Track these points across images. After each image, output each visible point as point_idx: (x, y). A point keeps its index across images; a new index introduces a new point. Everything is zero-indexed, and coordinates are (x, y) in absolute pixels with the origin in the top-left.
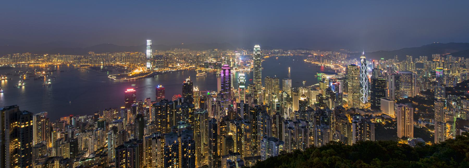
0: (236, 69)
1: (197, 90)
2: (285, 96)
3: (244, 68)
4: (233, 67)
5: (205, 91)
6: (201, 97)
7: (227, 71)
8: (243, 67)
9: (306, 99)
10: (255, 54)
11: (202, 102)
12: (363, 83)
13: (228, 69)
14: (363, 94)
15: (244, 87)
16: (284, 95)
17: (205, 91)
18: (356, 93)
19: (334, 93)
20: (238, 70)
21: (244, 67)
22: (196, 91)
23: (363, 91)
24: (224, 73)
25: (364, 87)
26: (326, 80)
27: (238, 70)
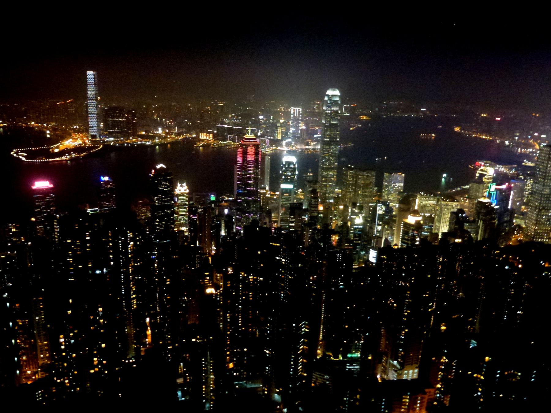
0: (288, 145)
1: (185, 190)
2: (381, 210)
3: (307, 144)
4: (282, 140)
5: (204, 194)
6: (192, 206)
7: (251, 150)
8: (306, 139)
9: (420, 221)
10: (327, 112)
11: (192, 216)
13: (254, 145)
15: (290, 186)
16: (378, 208)
17: (204, 194)
19: (496, 207)
20: (293, 146)
21: (307, 140)
22: (182, 191)
24: (245, 153)
26: (486, 177)
27: (294, 148)
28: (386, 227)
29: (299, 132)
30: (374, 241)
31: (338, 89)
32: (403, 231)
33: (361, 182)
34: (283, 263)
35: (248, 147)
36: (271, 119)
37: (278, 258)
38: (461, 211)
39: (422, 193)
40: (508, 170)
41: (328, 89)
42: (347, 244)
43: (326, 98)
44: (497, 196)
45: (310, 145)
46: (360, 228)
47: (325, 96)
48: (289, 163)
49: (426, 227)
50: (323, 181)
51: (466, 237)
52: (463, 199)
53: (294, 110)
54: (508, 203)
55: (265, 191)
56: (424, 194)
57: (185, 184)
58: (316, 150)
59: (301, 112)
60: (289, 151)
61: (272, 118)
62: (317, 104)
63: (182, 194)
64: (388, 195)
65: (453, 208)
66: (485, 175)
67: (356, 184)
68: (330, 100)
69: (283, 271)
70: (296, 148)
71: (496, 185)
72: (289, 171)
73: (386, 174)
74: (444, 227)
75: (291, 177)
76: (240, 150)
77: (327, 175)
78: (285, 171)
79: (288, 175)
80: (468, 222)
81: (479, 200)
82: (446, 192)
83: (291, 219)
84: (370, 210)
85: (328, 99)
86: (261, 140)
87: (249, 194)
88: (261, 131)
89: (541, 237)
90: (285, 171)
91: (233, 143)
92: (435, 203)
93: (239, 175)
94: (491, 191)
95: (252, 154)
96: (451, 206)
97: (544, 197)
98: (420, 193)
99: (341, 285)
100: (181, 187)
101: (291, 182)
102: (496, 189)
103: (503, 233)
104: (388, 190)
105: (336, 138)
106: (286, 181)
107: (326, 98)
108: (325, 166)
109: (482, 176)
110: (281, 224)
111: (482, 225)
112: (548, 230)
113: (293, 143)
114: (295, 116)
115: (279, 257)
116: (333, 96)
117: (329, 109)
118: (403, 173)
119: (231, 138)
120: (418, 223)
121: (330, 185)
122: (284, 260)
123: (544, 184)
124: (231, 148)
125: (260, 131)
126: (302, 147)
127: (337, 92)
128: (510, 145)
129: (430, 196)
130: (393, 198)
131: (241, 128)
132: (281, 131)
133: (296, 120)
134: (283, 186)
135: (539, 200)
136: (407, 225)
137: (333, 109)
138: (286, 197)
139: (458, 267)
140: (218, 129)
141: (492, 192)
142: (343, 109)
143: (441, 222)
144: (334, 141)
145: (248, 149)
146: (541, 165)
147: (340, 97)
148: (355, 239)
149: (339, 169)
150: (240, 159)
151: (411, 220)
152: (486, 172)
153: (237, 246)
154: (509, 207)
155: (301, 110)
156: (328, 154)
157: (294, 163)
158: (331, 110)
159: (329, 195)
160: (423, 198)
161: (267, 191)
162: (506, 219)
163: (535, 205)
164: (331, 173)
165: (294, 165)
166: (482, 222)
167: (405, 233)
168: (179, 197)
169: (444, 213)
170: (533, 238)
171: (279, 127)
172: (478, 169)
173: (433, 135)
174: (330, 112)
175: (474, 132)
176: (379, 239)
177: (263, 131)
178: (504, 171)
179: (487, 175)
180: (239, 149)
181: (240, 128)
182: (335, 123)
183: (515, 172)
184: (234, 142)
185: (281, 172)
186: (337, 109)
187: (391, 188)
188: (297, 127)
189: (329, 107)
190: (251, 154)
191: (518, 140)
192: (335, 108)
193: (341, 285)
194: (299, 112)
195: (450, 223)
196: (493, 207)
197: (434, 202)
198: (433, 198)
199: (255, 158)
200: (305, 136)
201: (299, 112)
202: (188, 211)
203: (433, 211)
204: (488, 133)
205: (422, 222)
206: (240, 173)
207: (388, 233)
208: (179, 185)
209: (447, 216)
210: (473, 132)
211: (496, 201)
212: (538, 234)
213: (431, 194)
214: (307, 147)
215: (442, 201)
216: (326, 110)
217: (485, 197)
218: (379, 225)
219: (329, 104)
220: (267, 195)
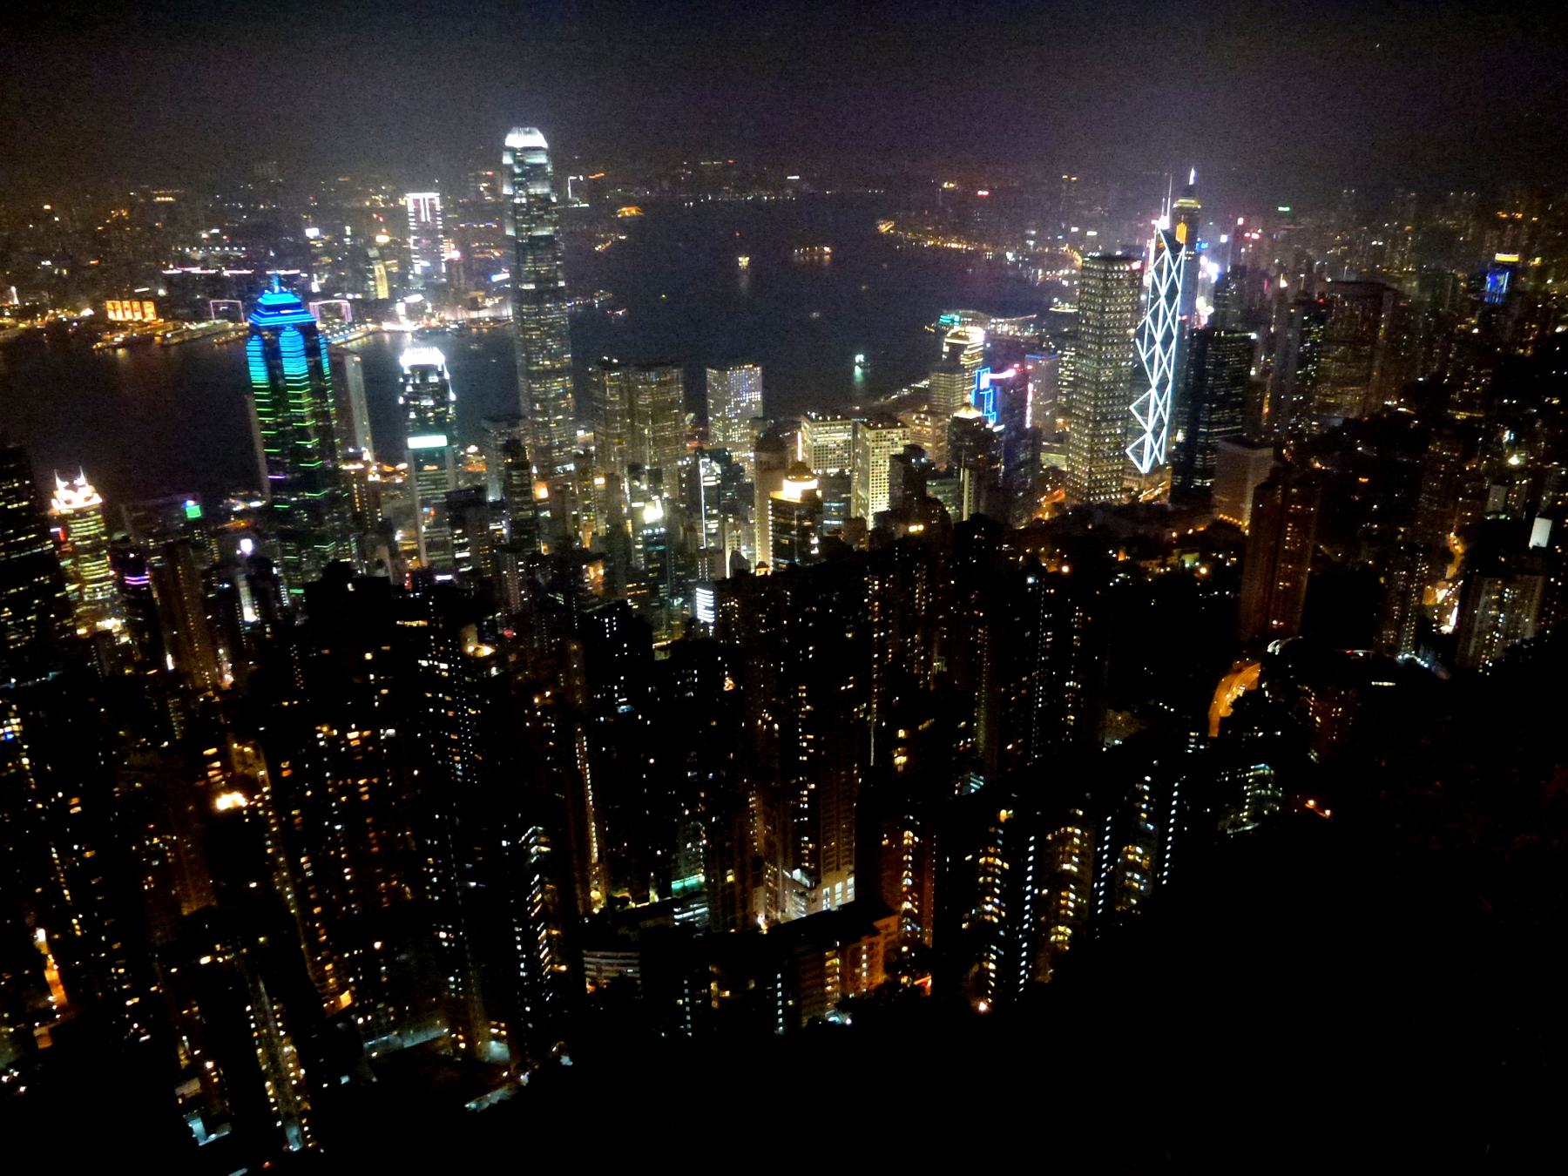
0: (414, 312)
1: (88, 499)
2: (709, 474)
3: (474, 305)
4: (390, 301)
6: (122, 547)
7: (290, 342)
8: (466, 291)
10: (517, 201)
11: (131, 580)
12: (1151, 360)
13: (295, 326)
15: (438, 441)
16: (702, 471)
18: (1112, 419)
19: (997, 429)
20: (432, 315)
21: (473, 294)
24: (272, 355)
25: (1154, 382)
26: (966, 352)
27: (434, 322)
28: (731, 520)
29: (444, 270)
30: (703, 565)
31: (541, 131)
32: (775, 524)
33: (645, 400)
34: (445, 674)
35: (278, 335)
36: (347, 237)
37: (424, 663)
38: (914, 450)
39: (813, 415)
40: (1019, 330)
41: (507, 130)
42: (630, 586)
43: (507, 160)
44: (998, 402)
45: (485, 308)
46: (660, 535)
47: (504, 153)
48: (424, 371)
50: (535, 413)
51: (933, 517)
52: (917, 418)
53: (416, 202)
54: (1023, 415)
55: (360, 466)
56: (817, 417)
57: (81, 480)
58: (504, 321)
59: (438, 208)
60: (421, 331)
61: (349, 233)
62: (487, 179)
63: (82, 514)
64: (725, 429)
65: (895, 444)
66: (964, 347)
67: (632, 412)
68: (521, 163)
69: (447, 698)
70: (440, 321)
71: (992, 372)
72: (427, 394)
73: (712, 373)
75: (437, 413)
76: (254, 347)
77: (546, 392)
78: (416, 395)
79: (426, 407)
80: (936, 476)
81: (956, 415)
82: (876, 403)
83: (458, 539)
84: (681, 481)
85: (515, 162)
86: (322, 305)
87: (310, 480)
88: (320, 278)
89: (1103, 490)
90: (416, 395)
91: (231, 325)
92: (850, 438)
93: (267, 427)
94: (982, 388)
95: (300, 353)
97: (1103, 390)
98: (806, 415)
99: (623, 703)
100: (71, 492)
101: (440, 426)
102: (993, 382)
103: (1021, 494)
104: (723, 418)
105: (556, 280)
106: (424, 427)
107: (507, 160)
108: (535, 368)
109: (957, 350)
110: (430, 559)
112: (1118, 471)
113: (429, 305)
114: (423, 220)
115: (427, 659)
116: (527, 150)
117: (521, 192)
118: (755, 366)
119: (221, 309)
120: (809, 496)
121: (558, 422)
122: (444, 666)
123: (1100, 357)
124: (227, 342)
125: (315, 276)
126: (459, 317)
127: (538, 139)
128: (1018, 261)
130: (739, 438)
131: (249, 272)
132: (383, 272)
133: (427, 231)
134: (416, 443)
136: (781, 508)
137: (532, 191)
138: (429, 475)
139: (920, 599)
140: (170, 282)
141: (985, 390)
142: (569, 189)
144: (548, 291)
145: (281, 339)
146: (1090, 309)
147: (549, 153)
148: (651, 567)
149: (576, 371)
150: (258, 374)
151: (791, 491)
152: (966, 338)
153: (295, 649)
154: (1028, 425)
155: (437, 202)
156: (538, 329)
157: (440, 369)
158: (528, 196)
159: (560, 452)
160: (815, 426)
161: (367, 464)
162: (1022, 456)
163: (1085, 411)
164: (556, 386)
165: (440, 374)
166: (967, 472)
167: (781, 529)
168: (72, 526)
171: (375, 259)
172: (947, 332)
173: (827, 249)
174: (524, 201)
176: (718, 557)
177: (326, 276)
178: (1008, 332)
180: (252, 343)
181: (246, 272)
182: (545, 233)
183: (1034, 332)
184: (235, 319)
185: (401, 401)
186: (546, 190)
187: (730, 410)
188: (435, 257)
189: (521, 185)
190: (294, 354)
191: (1035, 247)
192: (540, 189)
193: (623, 703)
194: (432, 207)
195: (892, 486)
196: (991, 430)
197: (846, 436)
199: (309, 367)
200: (462, 281)
201: (432, 207)
202: (113, 566)
204: (959, 231)
205: (819, 494)
206: (267, 420)
207: (738, 537)
208: (60, 484)
209: (882, 469)
210: (927, 234)
211: (995, 413)
212: (1096, 483)
213: (834, 414)
214: (474, 315)
215: (866, 430)
216: (513, 197)
217: (967, 405)
218: (710, 517)
219: (519, 175)
220: (371, 478)
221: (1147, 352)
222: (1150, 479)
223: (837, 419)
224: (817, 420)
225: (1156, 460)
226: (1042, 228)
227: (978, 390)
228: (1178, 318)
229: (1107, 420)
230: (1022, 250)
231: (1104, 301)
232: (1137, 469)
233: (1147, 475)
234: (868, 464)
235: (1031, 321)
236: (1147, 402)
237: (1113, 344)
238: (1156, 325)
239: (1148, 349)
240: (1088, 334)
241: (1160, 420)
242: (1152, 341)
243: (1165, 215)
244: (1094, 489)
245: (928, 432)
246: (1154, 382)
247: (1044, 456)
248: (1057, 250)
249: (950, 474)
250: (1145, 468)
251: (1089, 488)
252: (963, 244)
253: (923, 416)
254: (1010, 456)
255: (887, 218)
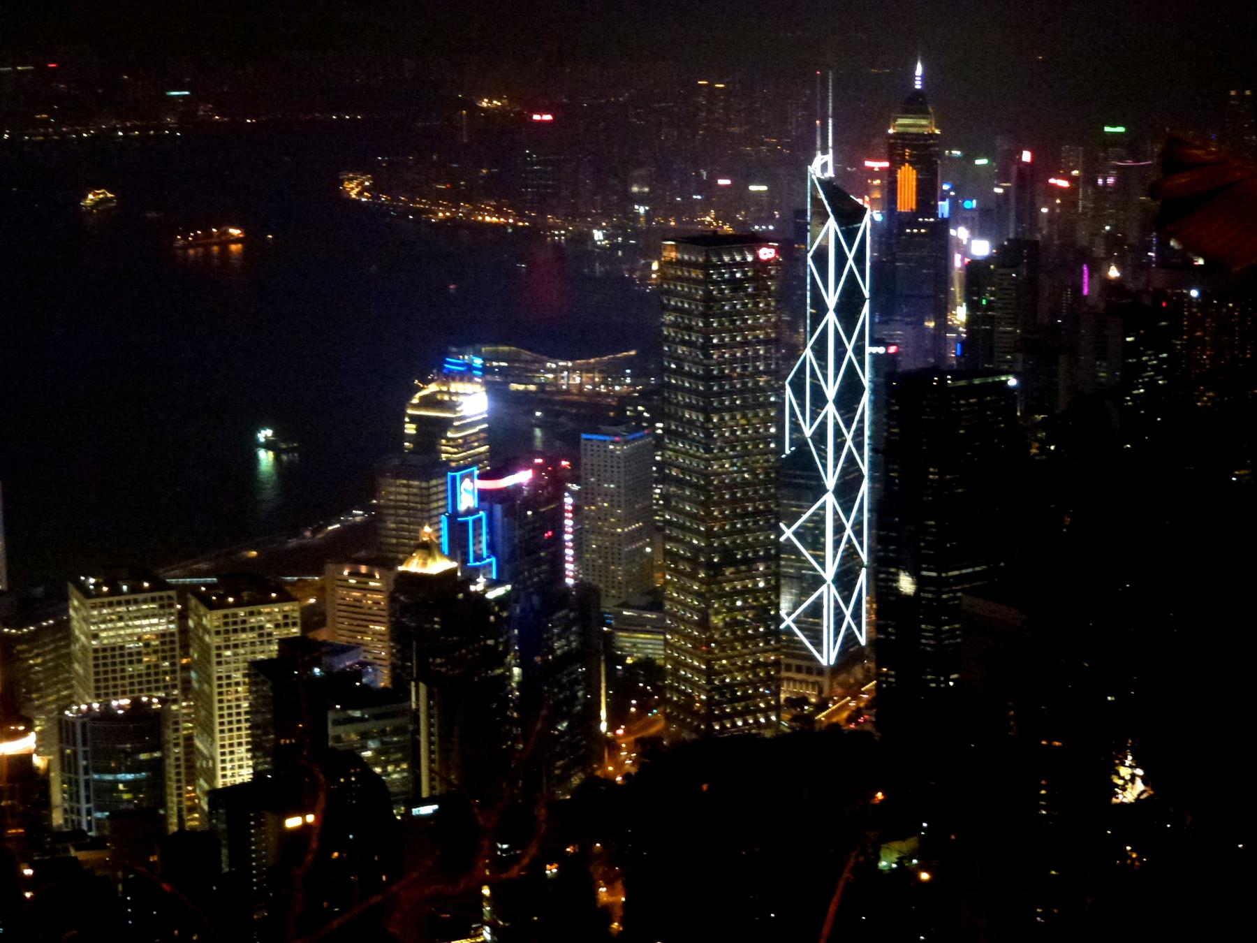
12: (820, 435)
14: (823, 565)
18: (745, 560)
23: (823, 520)
25: (830, 482)
39: (92, 580)
40: (604, 382)
49: (121, 776)
52: (351, 574)
54: (558, 560)
65: (264, 637)
66: (451, 421)
74: (236, 756)
81: (401, 568)
82: (293, 543)
94: (462, 507)
96: (252, 629)
102: (483, 495)
109: (432, 430)
111: (429, 708)
112: (765, 665)
128: (614, 247)
129: (116, 591)
135: (702, 520)
141: (469, 512)
143: (218, 728)
146: (683, 342)
160: (94, 607)
169: (220, 678)
170: (709, 718)
173: (235, 232)
175: (441, 194)
178: (581, 384)
179: (456, 424)
183: (633, 385)
196: (480, 596)
198: (153, 600)
203: (165, 673)
205: (39, 762)
215: (202, 610)
217: (428, 549)
221: (813, 419)
222: (842, 677)
223: (121, 593)
224: (100, 594)
225: (850, 638)
226: (660, 179)
227: (454, 516)
228: (869, 350)
229: (736, 563)
230: (624, 225)
231: (708, 324)
232: (813, 658)
233: (835, 670)
234: (210, 685)
235: (629, 362)
236: (819, 520)
237: (732, 409)
238: (824, 368)
239: (813, 419)
240: (683, 389)
241: (851, 554)
242: (819, 399)
243: (825, 152)
244: (719, 704)
245: (376, 603)
246: (830, 482)
247: (624, 639)
248: (691, 222)
249: (399, 690)
250: (828, 656)
251: (709, 703)
252: (507, 216)
253: (363, 569)
254: (532, 646)
255: (360, 168)
